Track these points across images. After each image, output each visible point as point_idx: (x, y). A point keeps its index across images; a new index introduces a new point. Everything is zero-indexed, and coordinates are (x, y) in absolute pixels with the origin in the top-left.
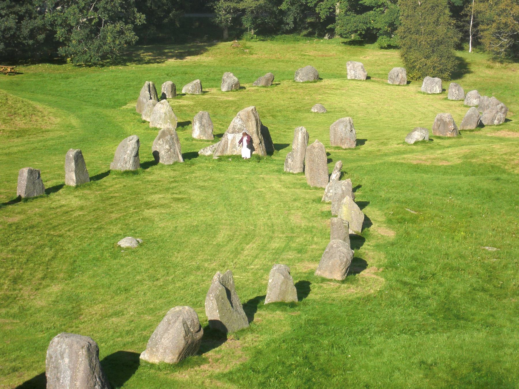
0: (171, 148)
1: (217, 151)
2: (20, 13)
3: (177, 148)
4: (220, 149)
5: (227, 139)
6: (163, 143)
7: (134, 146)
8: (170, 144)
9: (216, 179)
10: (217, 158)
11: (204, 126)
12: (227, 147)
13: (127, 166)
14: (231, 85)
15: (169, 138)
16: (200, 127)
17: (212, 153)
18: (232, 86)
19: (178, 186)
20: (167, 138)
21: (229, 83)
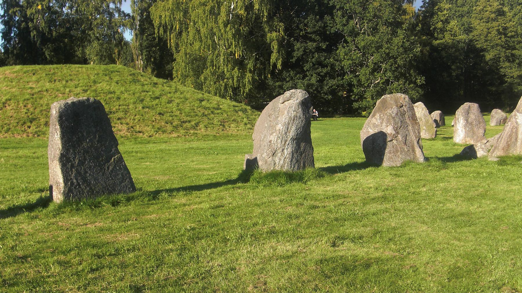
0: (398, 133)
1: (495, 148)
2: (321, 74)
3: (412, 133)
4: (502, 144)
5: (517, 123)
6: (382, 123)
7: (293, 114)
8: (395, 123)
9: (501, 196)
10: (496, 160)
11: (471, 124)
12: (516, 140)
13: (277, 161)
14: (499, 120)
15: (395, 112)
16: (465, 126)
17: (485, 154)
18: (500, 121)
19: (386, 211)
20: (389, 111)
21: (497, 119)
